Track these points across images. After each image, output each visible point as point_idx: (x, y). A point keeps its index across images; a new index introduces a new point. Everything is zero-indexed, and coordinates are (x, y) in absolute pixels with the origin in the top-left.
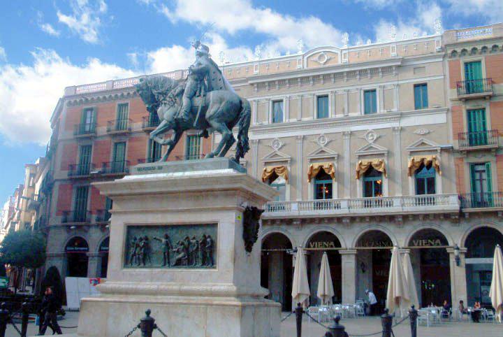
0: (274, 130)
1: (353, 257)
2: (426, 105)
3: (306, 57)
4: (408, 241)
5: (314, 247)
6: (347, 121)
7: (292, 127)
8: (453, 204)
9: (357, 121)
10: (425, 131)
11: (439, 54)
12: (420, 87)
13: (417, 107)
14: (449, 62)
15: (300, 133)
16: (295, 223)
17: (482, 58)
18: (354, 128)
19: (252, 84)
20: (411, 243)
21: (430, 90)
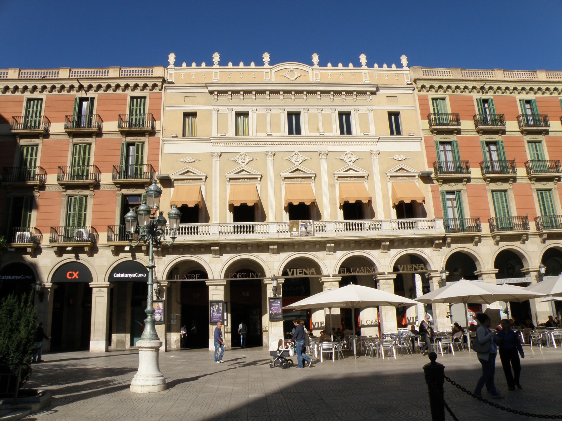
0: (239, 143)
1: (106, 290)
2: (399, 133)
3: (273, 71)
4: (393, 266)
5: (293, 274)
6: (322, 139)
7: (259, 141)
8: (439, 229)
9: (332, 140)
10: (402, 157)
11: (409, 86)
12: (394, 116)
13: (392, 133)
14: (419, 96)
15: (269, 149)
16: (271, 247)
17: (447, 95)
18: (330, 148)
19: (211, 92)
20: (396, 269)
21: (402, 119)
